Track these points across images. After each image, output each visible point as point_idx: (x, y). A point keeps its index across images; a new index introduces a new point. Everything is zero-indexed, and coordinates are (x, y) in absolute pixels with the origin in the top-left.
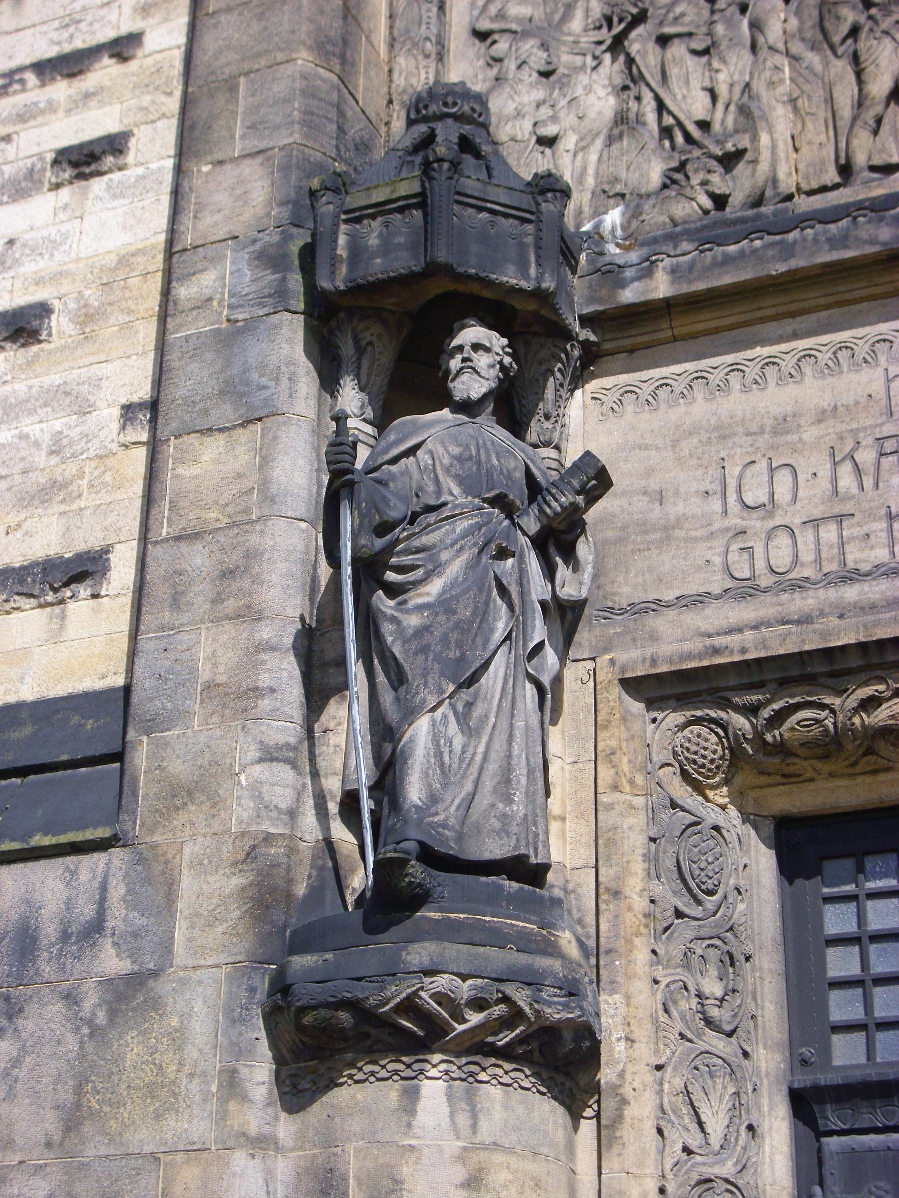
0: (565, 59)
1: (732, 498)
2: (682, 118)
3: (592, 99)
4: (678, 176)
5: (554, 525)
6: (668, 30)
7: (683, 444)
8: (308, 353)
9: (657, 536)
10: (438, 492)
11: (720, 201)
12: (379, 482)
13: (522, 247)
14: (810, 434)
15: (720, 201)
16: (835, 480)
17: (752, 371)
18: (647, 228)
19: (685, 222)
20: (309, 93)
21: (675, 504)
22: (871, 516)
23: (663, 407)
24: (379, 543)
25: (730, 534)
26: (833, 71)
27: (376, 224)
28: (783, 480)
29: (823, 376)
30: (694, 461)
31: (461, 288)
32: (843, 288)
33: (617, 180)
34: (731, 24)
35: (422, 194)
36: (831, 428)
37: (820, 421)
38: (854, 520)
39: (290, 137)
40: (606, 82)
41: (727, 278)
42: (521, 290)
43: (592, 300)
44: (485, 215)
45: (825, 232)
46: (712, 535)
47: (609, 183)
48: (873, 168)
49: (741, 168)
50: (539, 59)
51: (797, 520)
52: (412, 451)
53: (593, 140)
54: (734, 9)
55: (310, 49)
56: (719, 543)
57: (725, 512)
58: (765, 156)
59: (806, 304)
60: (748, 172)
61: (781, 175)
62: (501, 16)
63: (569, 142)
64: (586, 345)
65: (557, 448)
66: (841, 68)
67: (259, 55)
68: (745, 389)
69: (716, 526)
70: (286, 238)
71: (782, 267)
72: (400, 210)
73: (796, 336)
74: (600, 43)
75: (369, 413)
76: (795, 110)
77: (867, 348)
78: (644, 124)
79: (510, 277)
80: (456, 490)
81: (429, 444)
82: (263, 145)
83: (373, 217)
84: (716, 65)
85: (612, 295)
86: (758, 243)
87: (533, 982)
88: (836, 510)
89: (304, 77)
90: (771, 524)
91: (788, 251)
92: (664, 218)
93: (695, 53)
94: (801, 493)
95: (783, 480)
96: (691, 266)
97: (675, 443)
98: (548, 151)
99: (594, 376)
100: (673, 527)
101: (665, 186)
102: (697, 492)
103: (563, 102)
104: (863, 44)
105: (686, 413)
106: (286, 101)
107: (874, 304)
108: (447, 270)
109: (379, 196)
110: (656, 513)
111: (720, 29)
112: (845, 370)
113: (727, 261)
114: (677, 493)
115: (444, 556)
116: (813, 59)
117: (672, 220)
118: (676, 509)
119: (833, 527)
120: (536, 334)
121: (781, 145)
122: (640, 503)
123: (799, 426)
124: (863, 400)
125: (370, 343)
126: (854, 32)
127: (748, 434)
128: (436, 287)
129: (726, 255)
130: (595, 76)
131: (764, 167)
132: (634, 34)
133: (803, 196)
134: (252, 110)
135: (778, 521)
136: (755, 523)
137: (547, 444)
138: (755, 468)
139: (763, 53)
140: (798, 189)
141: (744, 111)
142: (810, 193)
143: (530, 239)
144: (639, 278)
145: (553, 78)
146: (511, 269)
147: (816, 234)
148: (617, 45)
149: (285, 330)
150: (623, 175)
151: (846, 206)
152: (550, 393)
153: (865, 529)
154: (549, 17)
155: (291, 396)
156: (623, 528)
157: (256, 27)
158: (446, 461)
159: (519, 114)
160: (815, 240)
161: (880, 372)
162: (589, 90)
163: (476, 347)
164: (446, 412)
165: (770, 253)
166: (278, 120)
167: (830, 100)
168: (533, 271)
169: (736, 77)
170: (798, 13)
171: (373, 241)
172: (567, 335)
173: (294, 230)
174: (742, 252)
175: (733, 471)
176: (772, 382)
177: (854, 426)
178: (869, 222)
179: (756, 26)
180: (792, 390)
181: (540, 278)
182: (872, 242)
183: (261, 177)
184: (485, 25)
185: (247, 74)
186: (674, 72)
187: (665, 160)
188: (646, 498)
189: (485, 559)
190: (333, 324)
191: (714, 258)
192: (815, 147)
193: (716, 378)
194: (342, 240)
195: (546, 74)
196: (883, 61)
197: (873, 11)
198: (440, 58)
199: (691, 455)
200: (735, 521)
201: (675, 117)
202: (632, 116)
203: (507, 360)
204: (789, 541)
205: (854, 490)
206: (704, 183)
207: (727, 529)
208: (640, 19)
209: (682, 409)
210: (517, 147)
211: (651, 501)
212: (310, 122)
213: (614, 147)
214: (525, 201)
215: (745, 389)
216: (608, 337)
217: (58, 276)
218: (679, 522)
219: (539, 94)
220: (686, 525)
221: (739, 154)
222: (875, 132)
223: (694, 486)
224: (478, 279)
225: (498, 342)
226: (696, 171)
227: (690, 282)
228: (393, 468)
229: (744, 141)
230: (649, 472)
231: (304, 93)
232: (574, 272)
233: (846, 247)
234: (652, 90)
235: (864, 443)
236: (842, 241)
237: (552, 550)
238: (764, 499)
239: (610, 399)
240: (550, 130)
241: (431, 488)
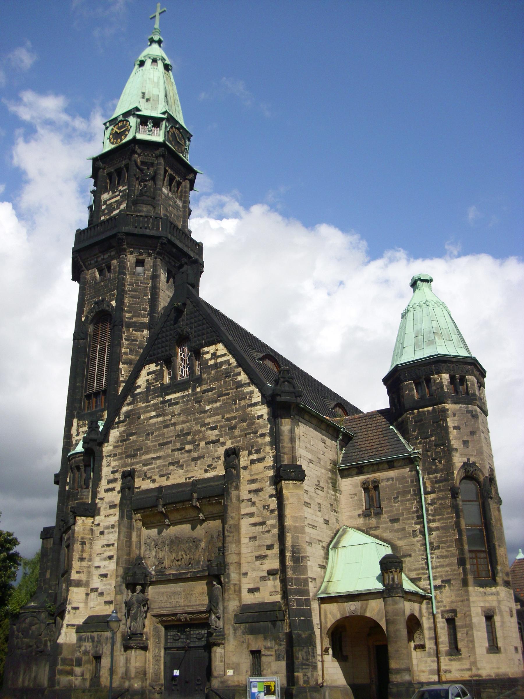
0: (151, 548)
39: (124, 565)
87: (139, 643)
91: (163, 578)
217: (108, 571)
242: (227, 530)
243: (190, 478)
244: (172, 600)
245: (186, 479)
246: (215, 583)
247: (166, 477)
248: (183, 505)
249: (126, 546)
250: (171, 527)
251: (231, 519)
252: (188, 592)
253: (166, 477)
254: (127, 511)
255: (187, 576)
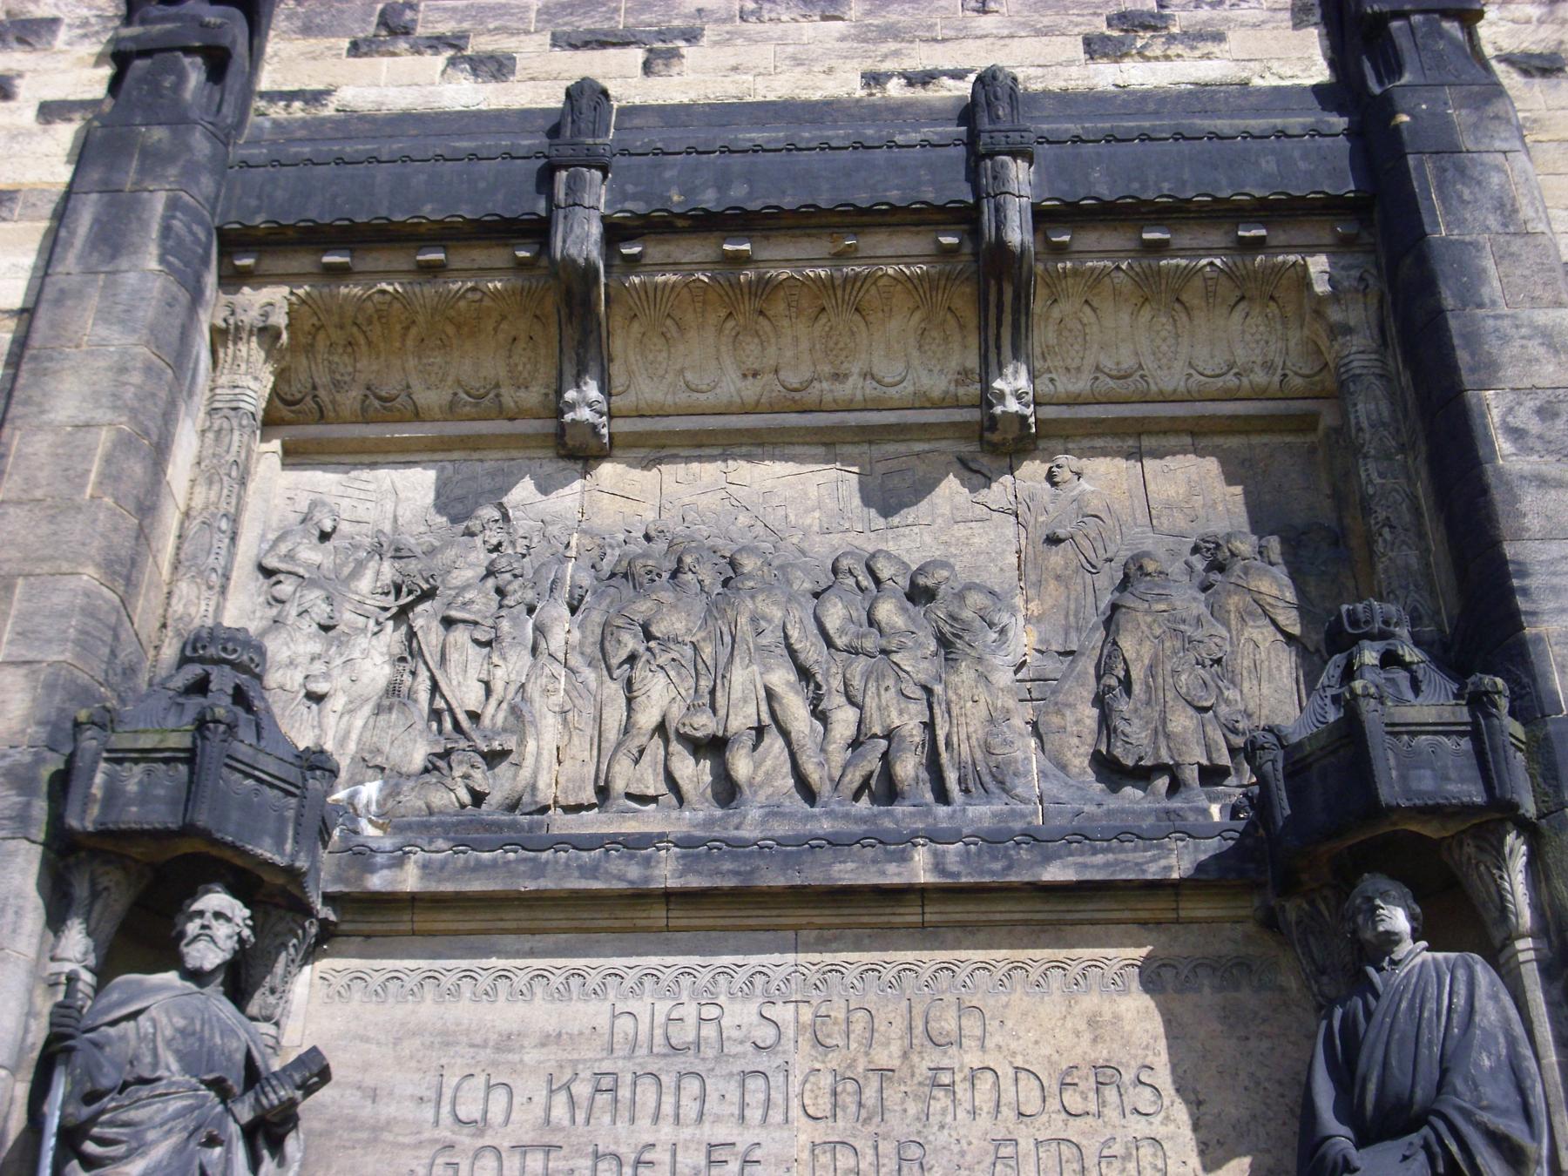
0: (347, 617)
1: (446, 1109)
2: (454, 705)
3: (368, 664)
4: (441, 764)
5: (269, 1117)
6: (454, 614)
7: (406, 1044)
8: (40, 887)
9: (364, 1135)
10: (155, 1065)
11: (478, 798)
12: (96, 1044)
13: (282, 820)
14: (531, 1056)
15: (478, 798)
16: (548, 1109)
17: (485, 981)
18: (403, 811)
19: (441, 812)
20: (89, 612)
21: (387, 1105)
22: (578, 1152)
23: (391, 1000)
24: (86, 1111)
25: (438, 1147)
26: (606, 692)
27: (138, 769)
28: (499, 1099)
29: (553, 1000)
30: (413, 1064)
31: (214, 852)
32: (585, 915)
33: (379, 751)
34: (515, 621)
35: (192, 751)
36: (552, 1055)
37: (543, 1045)
38: (562, 1153)
40: (385, 650)
41: (476, 885)
42: (273, 865)
43: (338, 879)
44: (250, 782)
45: (578, 858)
46: (419, 1145)
47: (371, 752)
48: (629, 796)
49: (503, 768)
50: (321, 611)
51: (506, 1144)
52: (133, 1016)
53: (361, 706)
54: (523, 608)
55: (98, 565)
56: (426, 1154)
57: (437, 1123)
58: (529, 762)
59: (548, 924)
60: (510, 774)
61: (541, 784)
62: (290, 556)
63: (337, 703)
64: (324, 923)
65: (277, 1024)
66: (614, 691)
67: (43, 560)
68: (475, 999)
69: (426, 1135)
70: (38, 760)
71: (530, 885)
72: (166, 761)
73: (532, 953)
74: (385, 609)
75: (92, 960)
76: (565, 721)
77: (598, 979)
78: (416, 701)
79: (266, 851)
80: (175, 1066)
81: (153, 1012)
82: (30, 656)
83: (136, 761)
84: (496, 659)
85: (360, 879)
86: (511, 855)
88: (546, 1140)
89: (87, 594)
90: (480, 1143)
91: (539, 870)
92: (421, 804)
93: (477, 642)
94: (514, 1116)
95: (499, 1099)
96: (443, 865)
97: (397, 1041)
98: (314, 707)
99: (326, 954)
100: (382, 1129)
101: (426, 770)
102: (412, 1096)
103: (339, 661)
104: (640, 672)
105: (413, 1012)
106: (63, 615)
107: (612, 936)
108: (205, 835)
109: (146, 742)
110: (367, 1111)
111: (505, 625)
112: (575, 996)
113: (479, 867)
114: (391, 1094)
115: (151, 1135)
116: (589, 675)
117: (429, 807)
118: (387, 1110)
119: (540, 1156)
120: (277, 906)
121: (545, 753)
122: (353, 1097)
123: (522, 1047)
124: (587, 1032)
125: (106, 889)
126: (632, 659)
127: (472, 1046)
128: (186, 847)
129: (478, 861)
130: (374, 641)
131: (525, 773)
132: (420, 609)
133: (559, 811)
134: (24, 616)
135: (487, 1141)
136: (465, 1140)
137: (267, 1019)
138: (472, 1082)
139: (544, 658)
140: (555, 802)
141: (515, 711)
142: (568, 809)
143: (290, 814)
144: (389, 867)
145: (331, 634)
146: (268, 841)
147: (568, 859)
148: (402, 615)
149: (20, 860)
150: (386, 748)
151: (603, 836)
152: (279, 967)
153: (571, 1164)
154: (337, 568)
155: (14, 931)
156: (331, 1121)
157: (45, 529)
158: (169, 1033)
159: (292, 663)
160: (567, 865)
161: (607, 1006)
162: (366, 654)
163: (218, 915)
164: (171, 977)
165: (522, 868)
166: (52, 633)
167: (599, 720)
168: (289, 847)
169: (513, 677)
170: (581, 626)
171: (132, 787)
172: (308, 912)
173: (49, 754)
174: (495, 861)
175: (451, 1081)
176: (502, 996)
177: (576, 1056)
178: (620, 857)
179: (540, 630)
180: (520, 1008)
181: (294, 856)
182: (620, 878)
183: (23, 690)
184: (272, 562)
185: (27, 576)
186: (454, 657)
187: (430, 743)
188: (359, 1094)
189: (192, 1144)
190: (72, 860)
191: (467, 861)
192: (579, 763)
193: (448, 981)
194: (99, 778)
195: (325, 628)
196: (655, 695)
197: (652, 644)
198: (223, 590)
199: (412, 1057)
200: (445, 1133)
201: (447, 702)
202: (404, 689)
203: (246, 932)
204: (495, 1164)
205: (566, 1122)
206: (466, 777)
207: (436, 1141)
208: (428, 595)
209: (410, 1006)
210: (285, 696)
211: (364, 1097)
212: (84, 643)
213: (381, 717)
214: (293, 774)
215: (475, 999)
216: (348, 917)
218: (389, 1125)
219: (316, 647)
220: (396, 1129)
221: (505, 754)
222: (637, 762)
223: (410, 1090)
224: (233, 847)
225: (240, 911)
226: (461, 763)
227: (439, 881)
228: (112, 1031)
229: (511, 743)
230: (366, 1067)
231: (83, 610)
232: (325, 847)
233: (596, 878)
234: (429, 669)
235: (582, 1075)
236: (592, 871)
237: (261, 1142)
238: (477, 1115)
239: (339, 981)
240: (320, 687)
241: (148, 1059)
242: (1516, 434)
243: (926, 78)
244: (645, 1132)
245: (874, 79)
246: (1397, 919)
247: (637, 55)
248: (841, 256)
249: (110, 477)
250: (607, 471)
251: (1536, 348)
252: (887, 1056)
253: (637, 55)
254: (173, 205)
255: (893, 875)
